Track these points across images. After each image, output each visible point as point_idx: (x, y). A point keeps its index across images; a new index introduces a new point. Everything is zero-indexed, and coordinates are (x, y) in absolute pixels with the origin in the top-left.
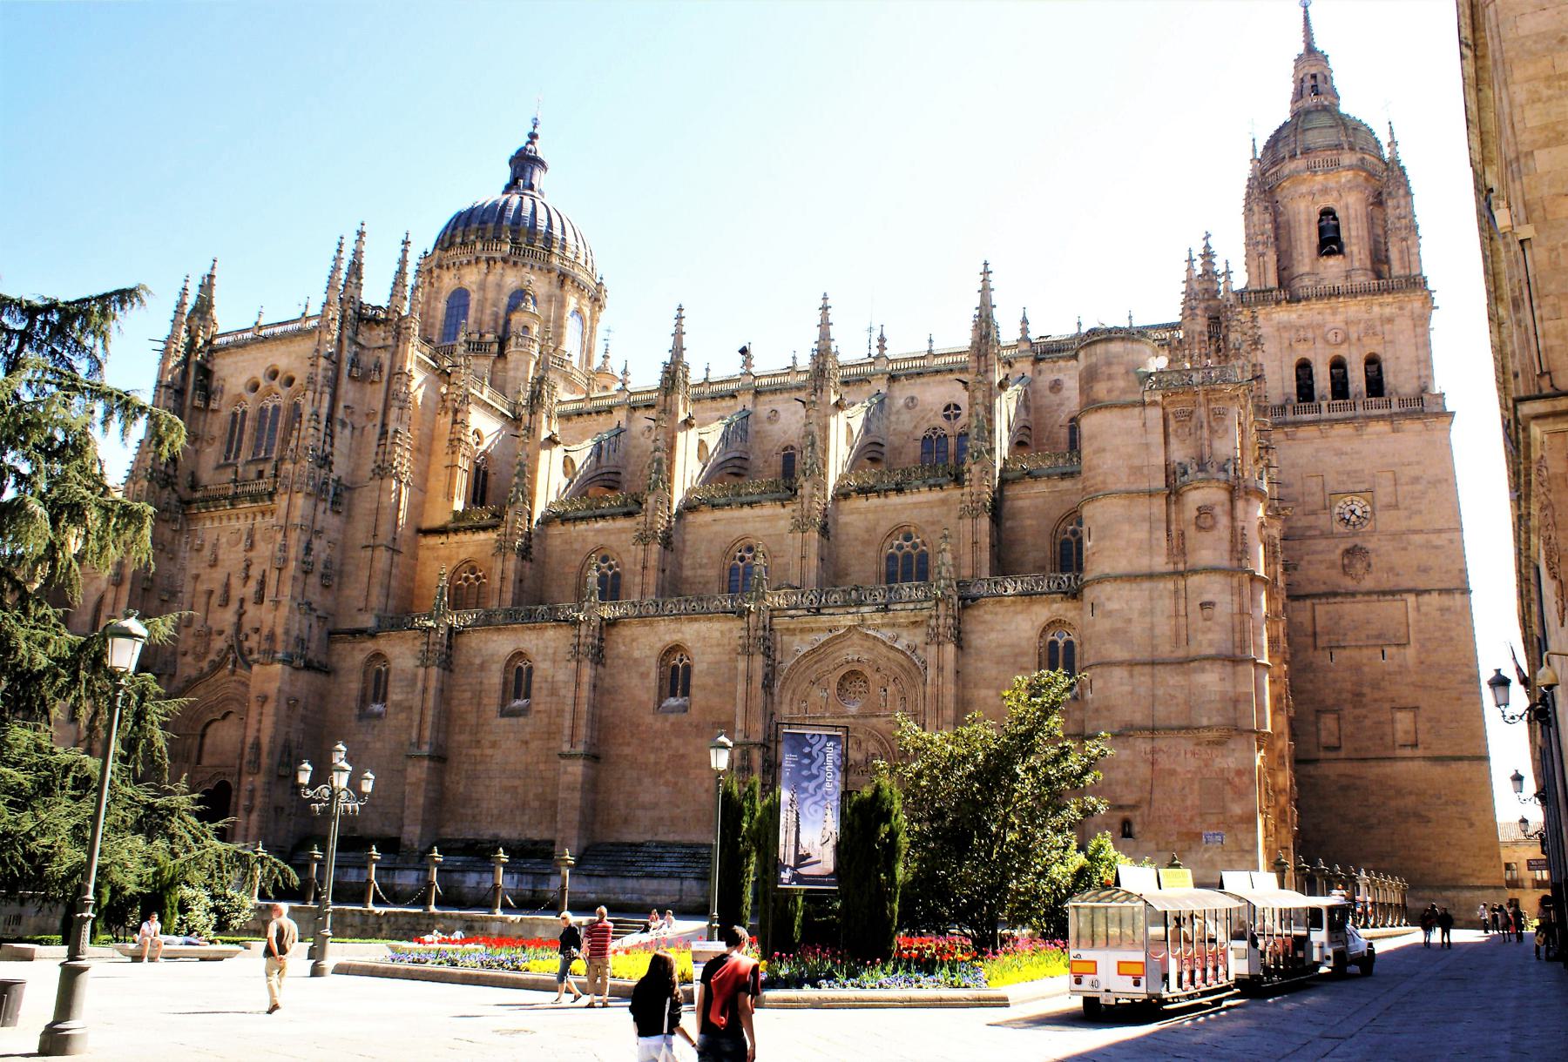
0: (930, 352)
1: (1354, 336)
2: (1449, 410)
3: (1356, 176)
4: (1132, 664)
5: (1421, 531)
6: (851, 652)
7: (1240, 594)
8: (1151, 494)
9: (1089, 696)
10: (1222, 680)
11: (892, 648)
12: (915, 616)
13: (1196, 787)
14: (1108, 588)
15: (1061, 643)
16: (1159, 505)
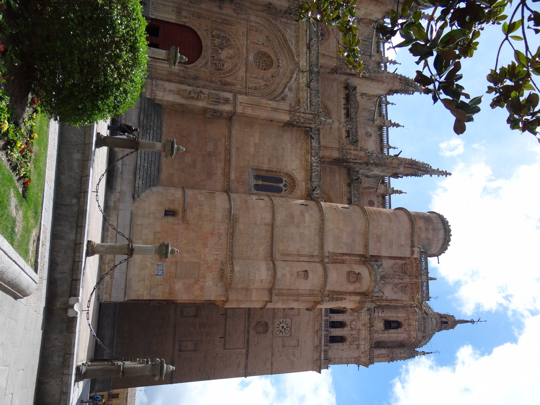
0: (390, 147)
1: (353, 332)
2: (322, 370)
3: (414, 338)
4: (272, 225)
5: (272, 357)
6: (284, 63)
7: (310, 295)
8: (366, 246)
9: (254, 197)
10: (261, 281)
11: (285, 87)
12: (304, 102)
13: (195, 260)
14: (317, 215)
15: (281, 185)
16: (360, 250)
